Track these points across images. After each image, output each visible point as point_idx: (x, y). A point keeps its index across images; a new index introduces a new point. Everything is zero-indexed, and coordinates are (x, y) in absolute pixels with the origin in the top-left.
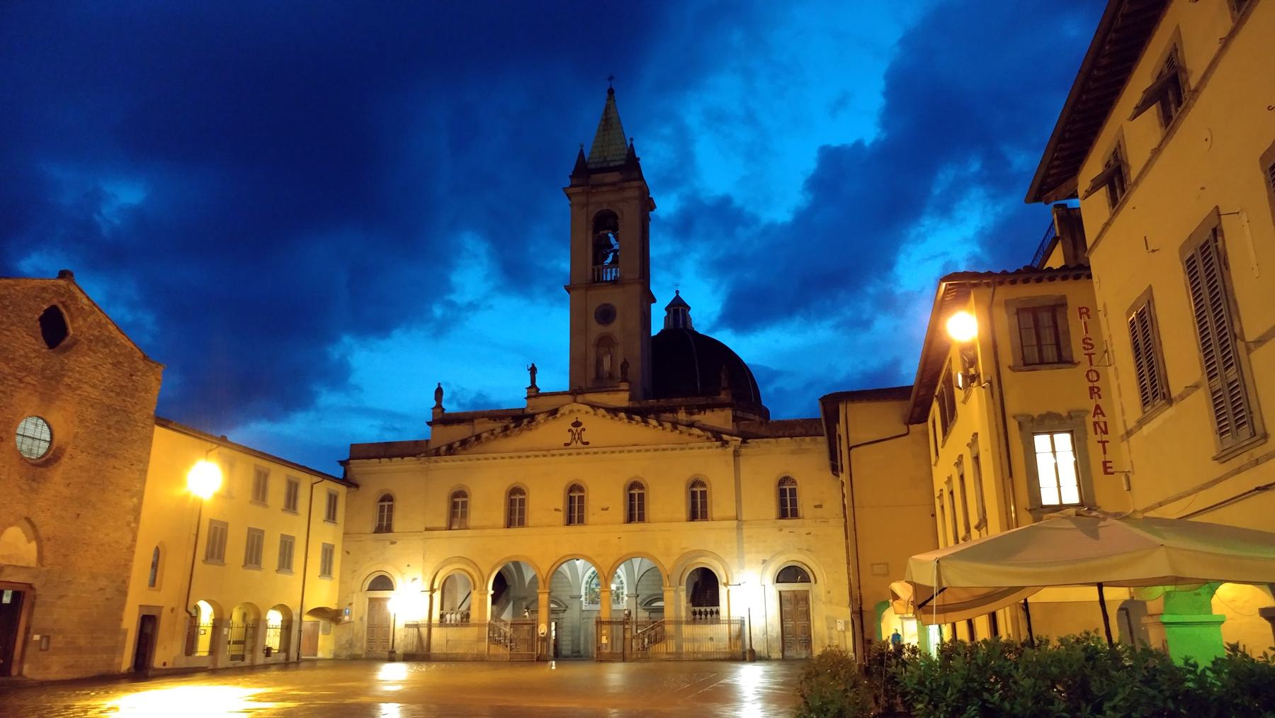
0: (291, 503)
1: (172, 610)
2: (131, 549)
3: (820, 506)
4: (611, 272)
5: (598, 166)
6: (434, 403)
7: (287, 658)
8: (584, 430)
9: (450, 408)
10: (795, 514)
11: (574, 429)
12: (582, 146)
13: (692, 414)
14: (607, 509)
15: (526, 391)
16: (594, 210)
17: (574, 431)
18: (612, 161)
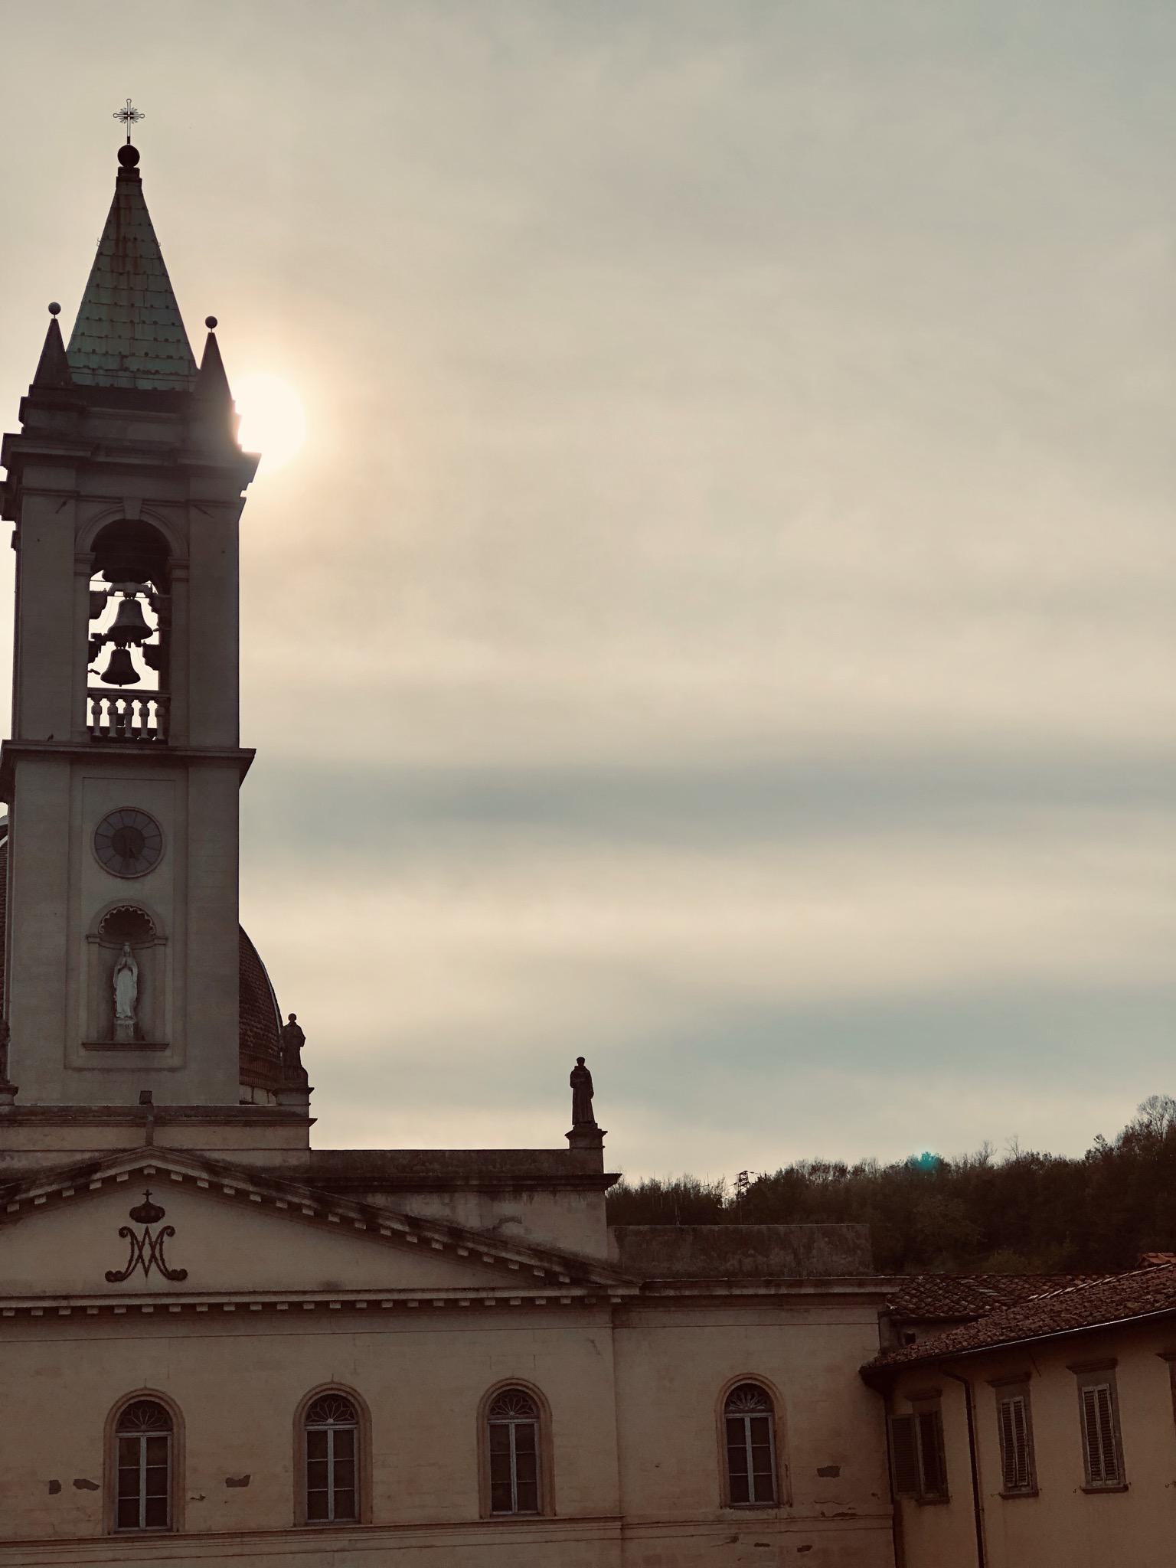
3: (831, 1472)
5: (104, 382)
8: (170, 1231)
10: (769, 1493)
11: (139, 1229)
12: (55, 309)
14: (244, 1482)
17: (140, 1239)
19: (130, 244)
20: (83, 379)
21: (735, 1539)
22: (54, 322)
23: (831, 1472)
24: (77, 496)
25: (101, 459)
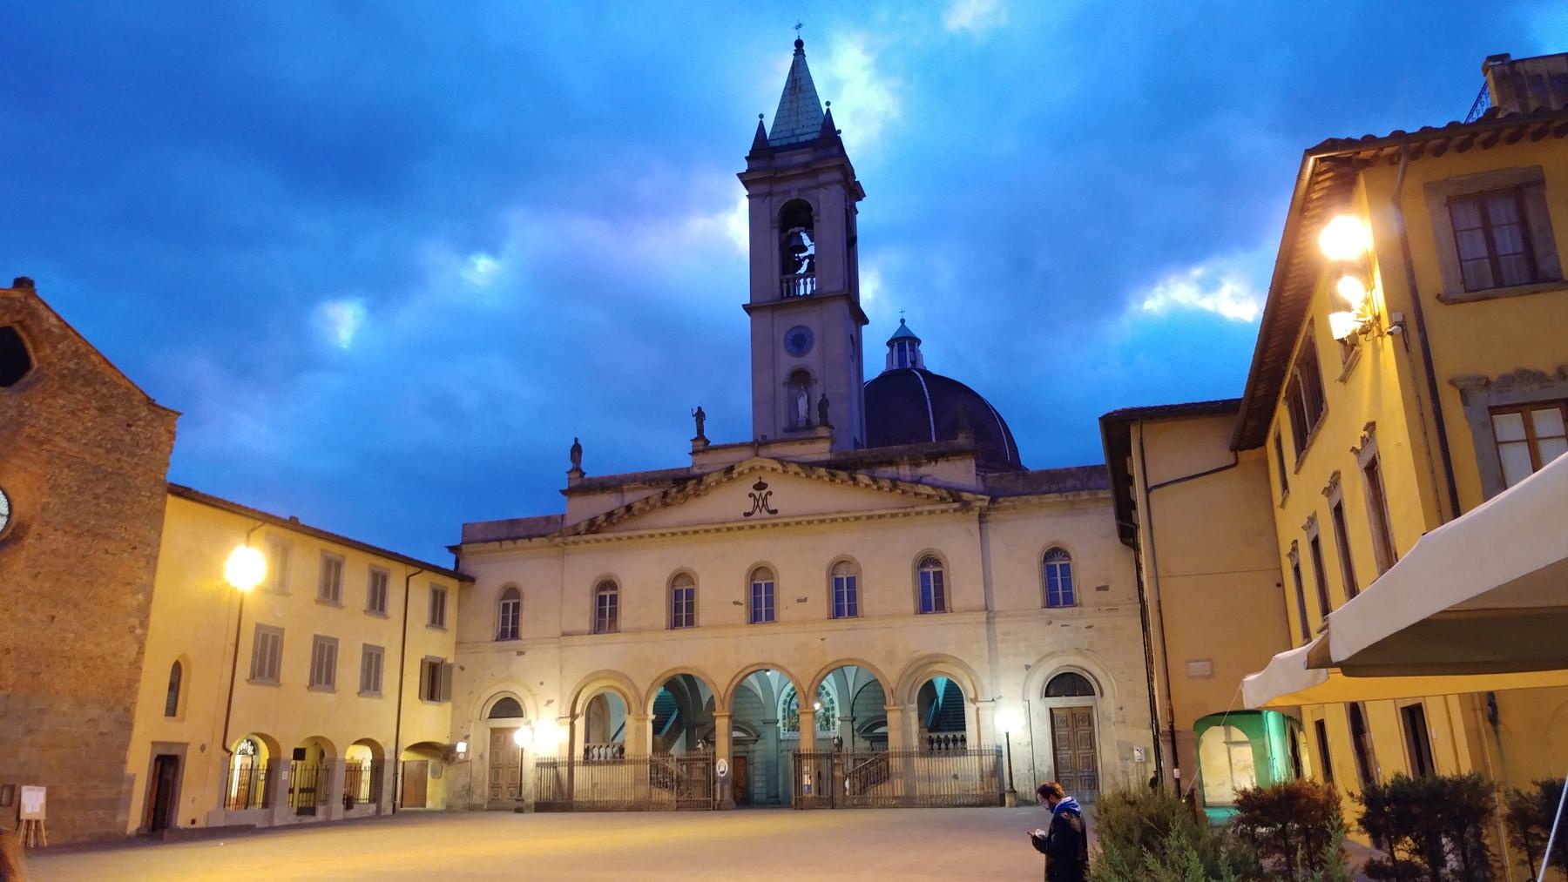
0: (377, 603)
1: (203, 748)
2: (136, 665)
3: (1105, 588)
4: (805, 284)
5: (785, 142)
6: (570, 466)
7: (379, 810)
9: (593, 468)
10: (1069, 601)
11: (757, 493)
13: (918, 465)
14: (805, 600)
15: (691, 444)
16: (778, 203)
17: (758, 497)
18: (802, 134)
19: (798, 82)
20: (773, 144)
21: (1051, 623)
22: (761, 122)
23: (1105, 588)
24: (770, 194)
25: (779, 175)
